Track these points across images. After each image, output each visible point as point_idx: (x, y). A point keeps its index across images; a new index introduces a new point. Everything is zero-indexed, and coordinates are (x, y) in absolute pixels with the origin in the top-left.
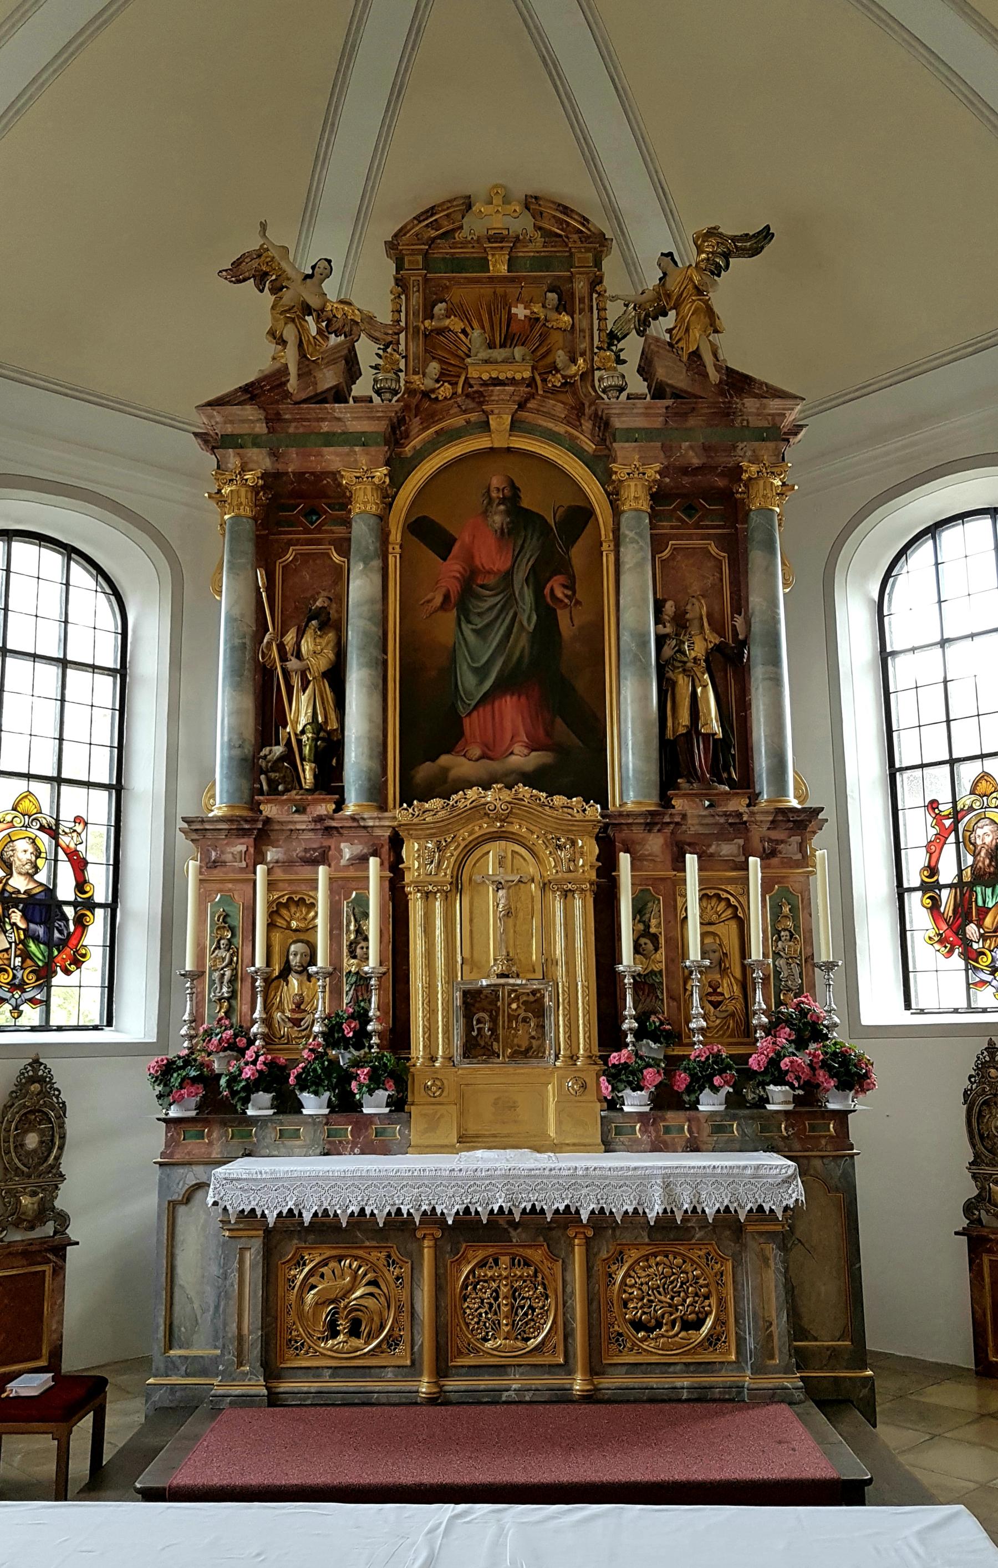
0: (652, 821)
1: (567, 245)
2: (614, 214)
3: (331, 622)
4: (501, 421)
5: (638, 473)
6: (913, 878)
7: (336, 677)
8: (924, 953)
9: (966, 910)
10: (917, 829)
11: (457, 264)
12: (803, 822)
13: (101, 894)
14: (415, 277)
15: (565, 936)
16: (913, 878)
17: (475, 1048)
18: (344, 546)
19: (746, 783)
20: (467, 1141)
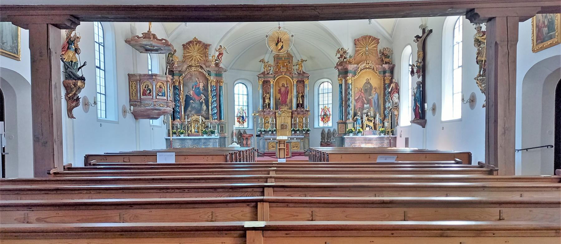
1: (289, 57)
8: (320, 121)
9: (323, 118)
10: (320, 110)
11: (280, 59)
15: (289, 120)
18: (270, 86)
19: (304, 108)
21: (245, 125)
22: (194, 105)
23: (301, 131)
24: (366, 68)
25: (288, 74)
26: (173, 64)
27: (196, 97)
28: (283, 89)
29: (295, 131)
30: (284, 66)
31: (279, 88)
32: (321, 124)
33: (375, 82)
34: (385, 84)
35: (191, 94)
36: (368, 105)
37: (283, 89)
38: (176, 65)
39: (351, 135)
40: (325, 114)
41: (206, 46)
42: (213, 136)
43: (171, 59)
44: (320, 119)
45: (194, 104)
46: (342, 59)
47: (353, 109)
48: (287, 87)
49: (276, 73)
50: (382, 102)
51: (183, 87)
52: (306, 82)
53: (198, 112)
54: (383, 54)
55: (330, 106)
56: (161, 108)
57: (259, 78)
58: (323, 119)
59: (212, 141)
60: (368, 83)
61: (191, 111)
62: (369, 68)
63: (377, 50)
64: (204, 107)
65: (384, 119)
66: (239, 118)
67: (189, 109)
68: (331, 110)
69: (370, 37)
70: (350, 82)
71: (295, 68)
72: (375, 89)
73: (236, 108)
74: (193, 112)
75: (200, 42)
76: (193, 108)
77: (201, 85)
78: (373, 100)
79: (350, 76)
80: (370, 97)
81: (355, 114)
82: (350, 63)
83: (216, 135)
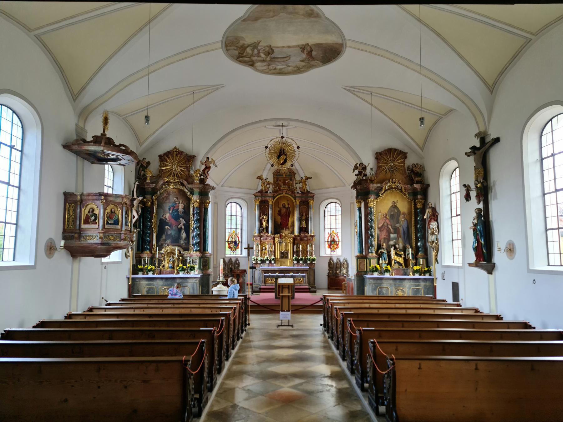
0: (298, 236)
1: (292, 174)
2: (297, 170)
3: (267, 215)
4: (284, 193)
5: (298, 202)
6: (326, 240)
7: (268, 221)
9: (331, 244)
10: (327, 235)
12: (313, 236)
13: (240, 240)
14: (276, 177)
15: (290, 247)
16: (326, 240)
17: (282, 257)
18: (268, 206)
19: (308, 232)
20: (281, 265)
21: (238, 251)
22: (169, 232)
23: (305, 261)
24: (392, 188)
25: (290, 193)
26: (146, 179)
27: (173, 221)
28: (284, 210)
29: (298, 261)
30: (285, 184)
31: (278, 209)
32: (328, 251)
33: (403, 206)
34: (416, 209)
35: (167, 217)
36: (395, 235)
37: (284, 210)
38: (148, 181)
39: (376, 275)
40: (334, 240)
41: (189, 159)
42: (192, 274)
43: (143, 173)
44: (327, 245)
45: (170, 231)
46: (360, 177)
47: (376, 240)
48: (289, 208)
49: (275, 191)
51: (157, 209)
52: (311, 203)
53: (176, 241)
54: (412, 170)
55: (339, 231)
56: (111, 242)
57: (256, 196)
58: (329, 246)
59: (190, 280)
60: (394, 206)
61: (165, 240)
62: (395, 188)
63: (404, 166)
64: (184, 235)
65: (417, 253)
66: (230, 243)
67: (164, 237)
68: (340, 235)
69: (395, 150)
70: (372, 205)
71: (298, 186)
72: (404, 214)
73: (228, 231)
74: (168, 241)
75: (181, 153)
76: (168, 236)
77: (181, 207)
78: (401, 229)
79: (372, 197)
80: (398, 225)
81: (379, 247)
82: (372, 181)
83: (196, 273)
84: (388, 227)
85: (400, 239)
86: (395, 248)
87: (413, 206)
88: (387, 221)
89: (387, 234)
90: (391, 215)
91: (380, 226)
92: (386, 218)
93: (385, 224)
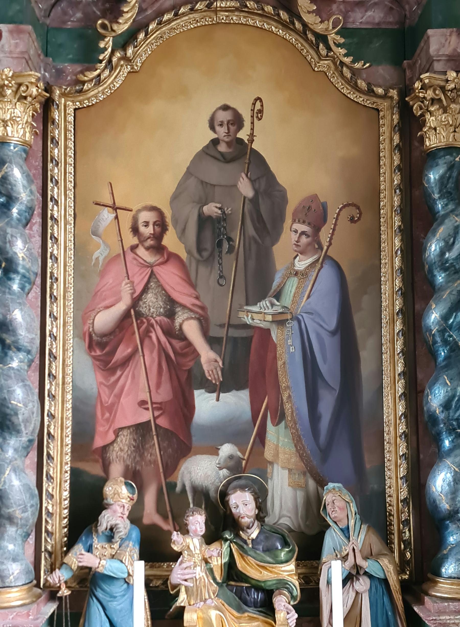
36: (236, 402)
50: (393, 367)
60: (232, 149)
72: (315, 214)
78: (287, 346)
80: (259, 314)
84: (174, 334)
85: (278, 439)
86: (222, 524)
87: (389, 138)
88: (169, 276)
89: (164, 394)
90: (203, 221)
91: (104, 319)
92: (158, 248)
93: (152, 303)
